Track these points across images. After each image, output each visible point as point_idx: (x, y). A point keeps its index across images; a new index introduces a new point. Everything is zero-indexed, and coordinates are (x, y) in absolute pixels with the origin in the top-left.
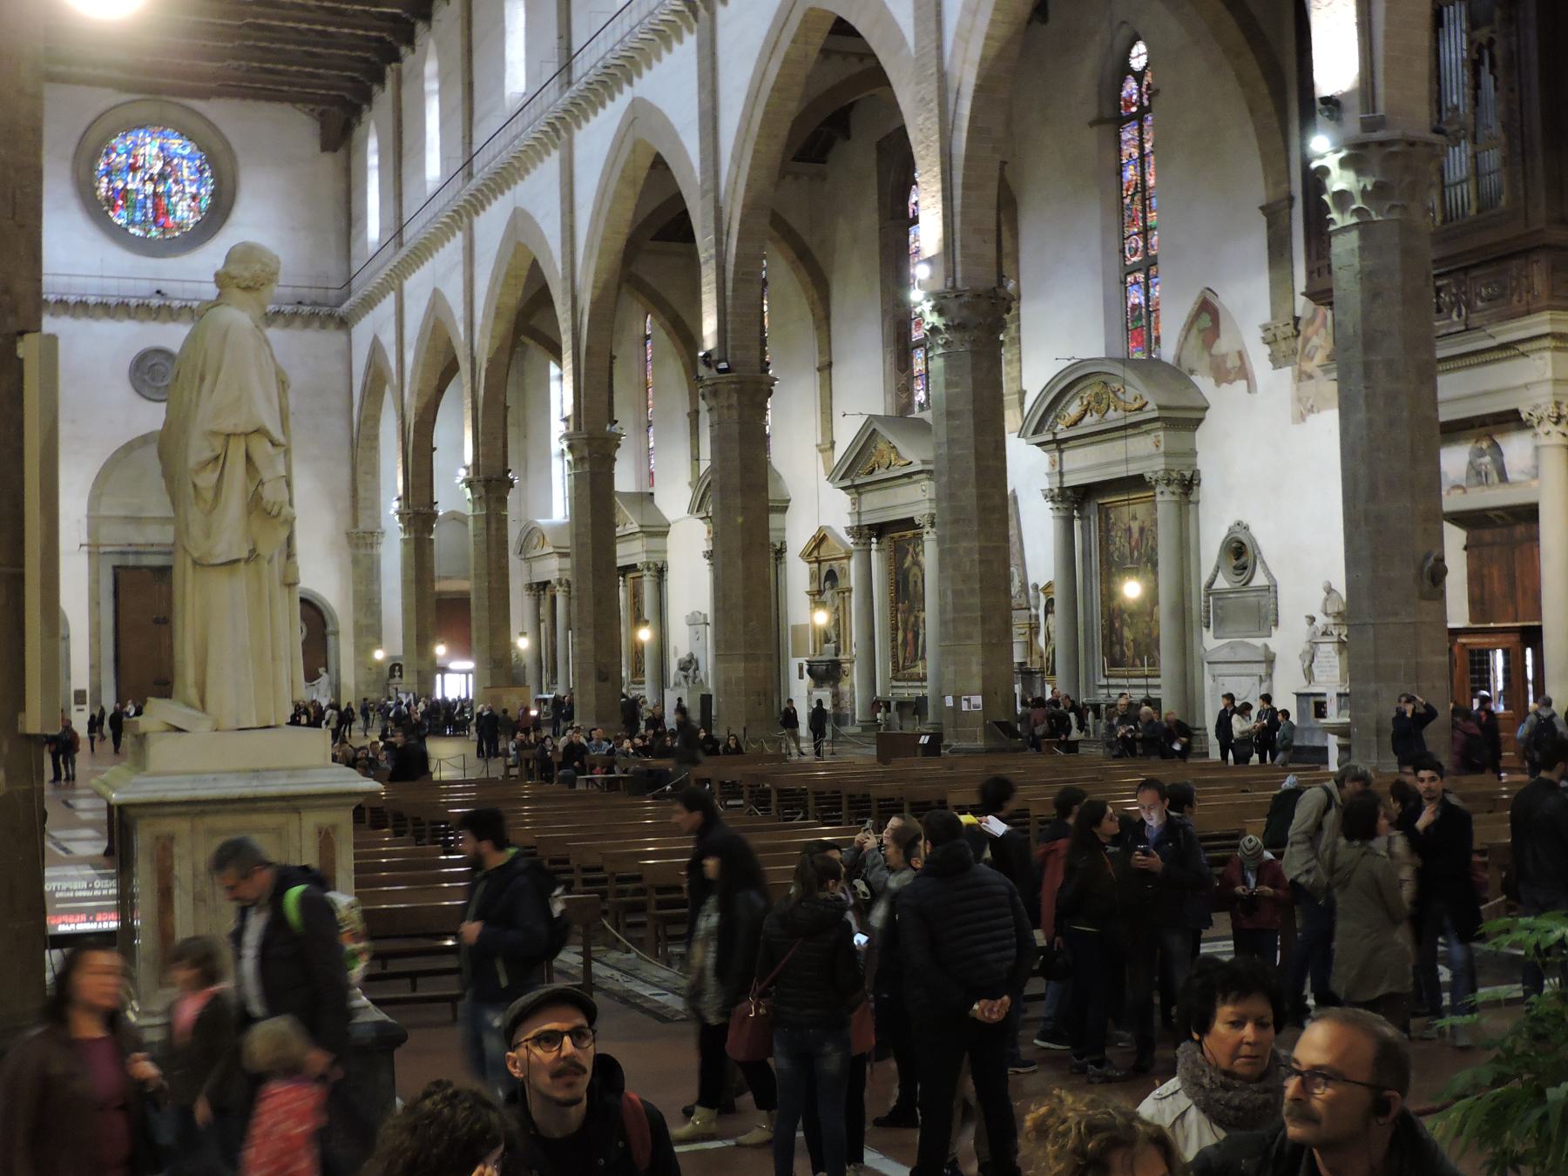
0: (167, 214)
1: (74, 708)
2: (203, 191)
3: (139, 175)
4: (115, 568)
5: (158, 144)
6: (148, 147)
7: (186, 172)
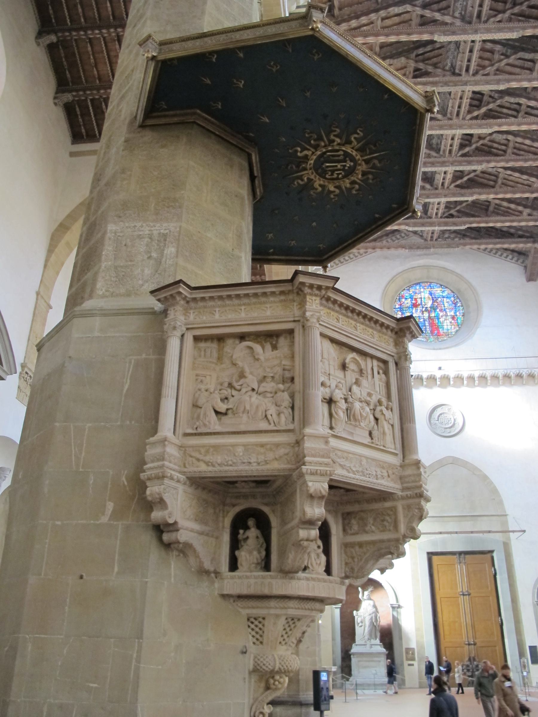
0: (438, 329)
1: (406, 663)
2: (458, 313)
3: (419, 308)
4: (430, 555)
5: (428, 292)
6: (422, 294)
7: (446, 305)
